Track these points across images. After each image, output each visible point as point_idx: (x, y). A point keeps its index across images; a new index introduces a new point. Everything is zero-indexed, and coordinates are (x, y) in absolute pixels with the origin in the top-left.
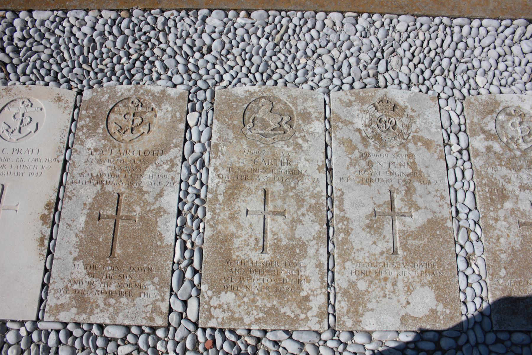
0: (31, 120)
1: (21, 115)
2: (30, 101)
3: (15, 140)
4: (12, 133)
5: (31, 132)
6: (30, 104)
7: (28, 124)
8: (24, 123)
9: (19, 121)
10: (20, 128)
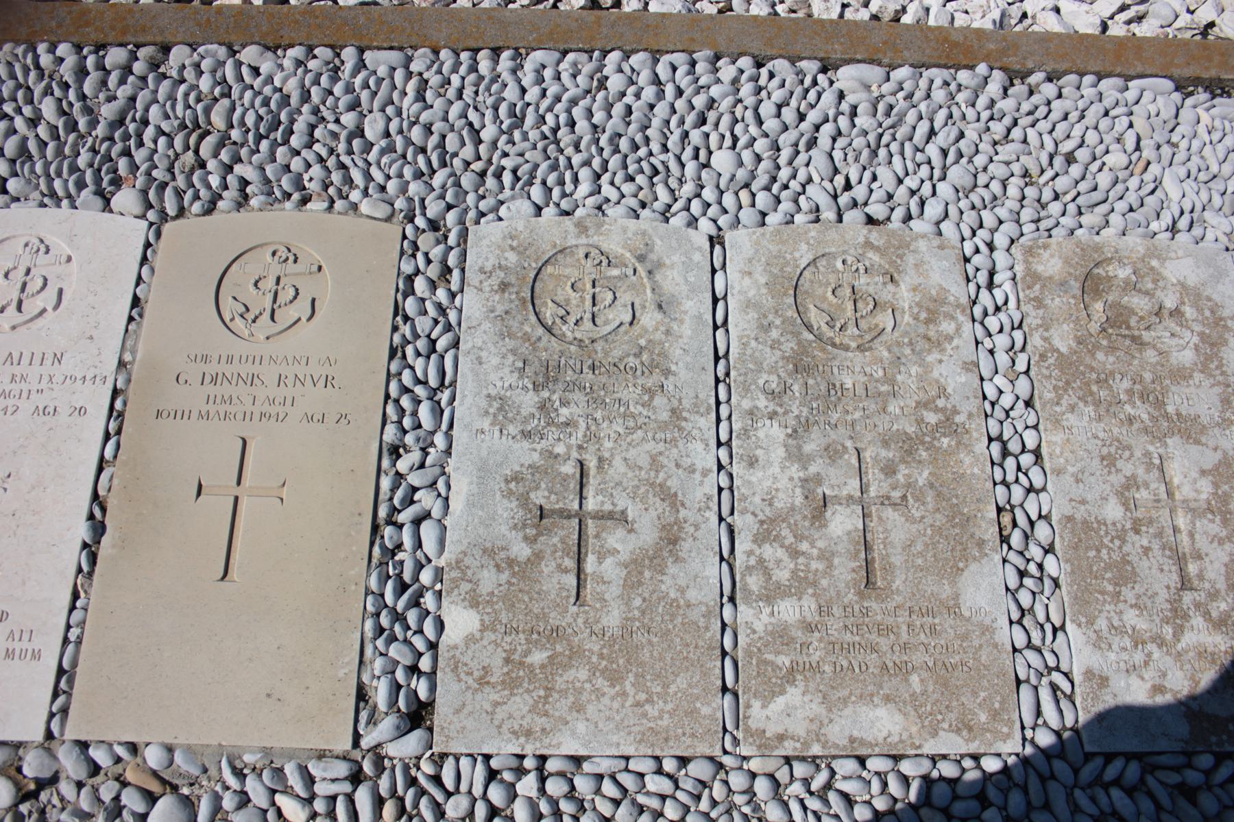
0: (297, 293)
2: (289, 250)
3: (262, 337)
4: (254, 321)
5: (299, 319)
6: (292, 258)
7: (291, 302)
8: (281, 300)
9: (270, 297)
10: (273, 311)
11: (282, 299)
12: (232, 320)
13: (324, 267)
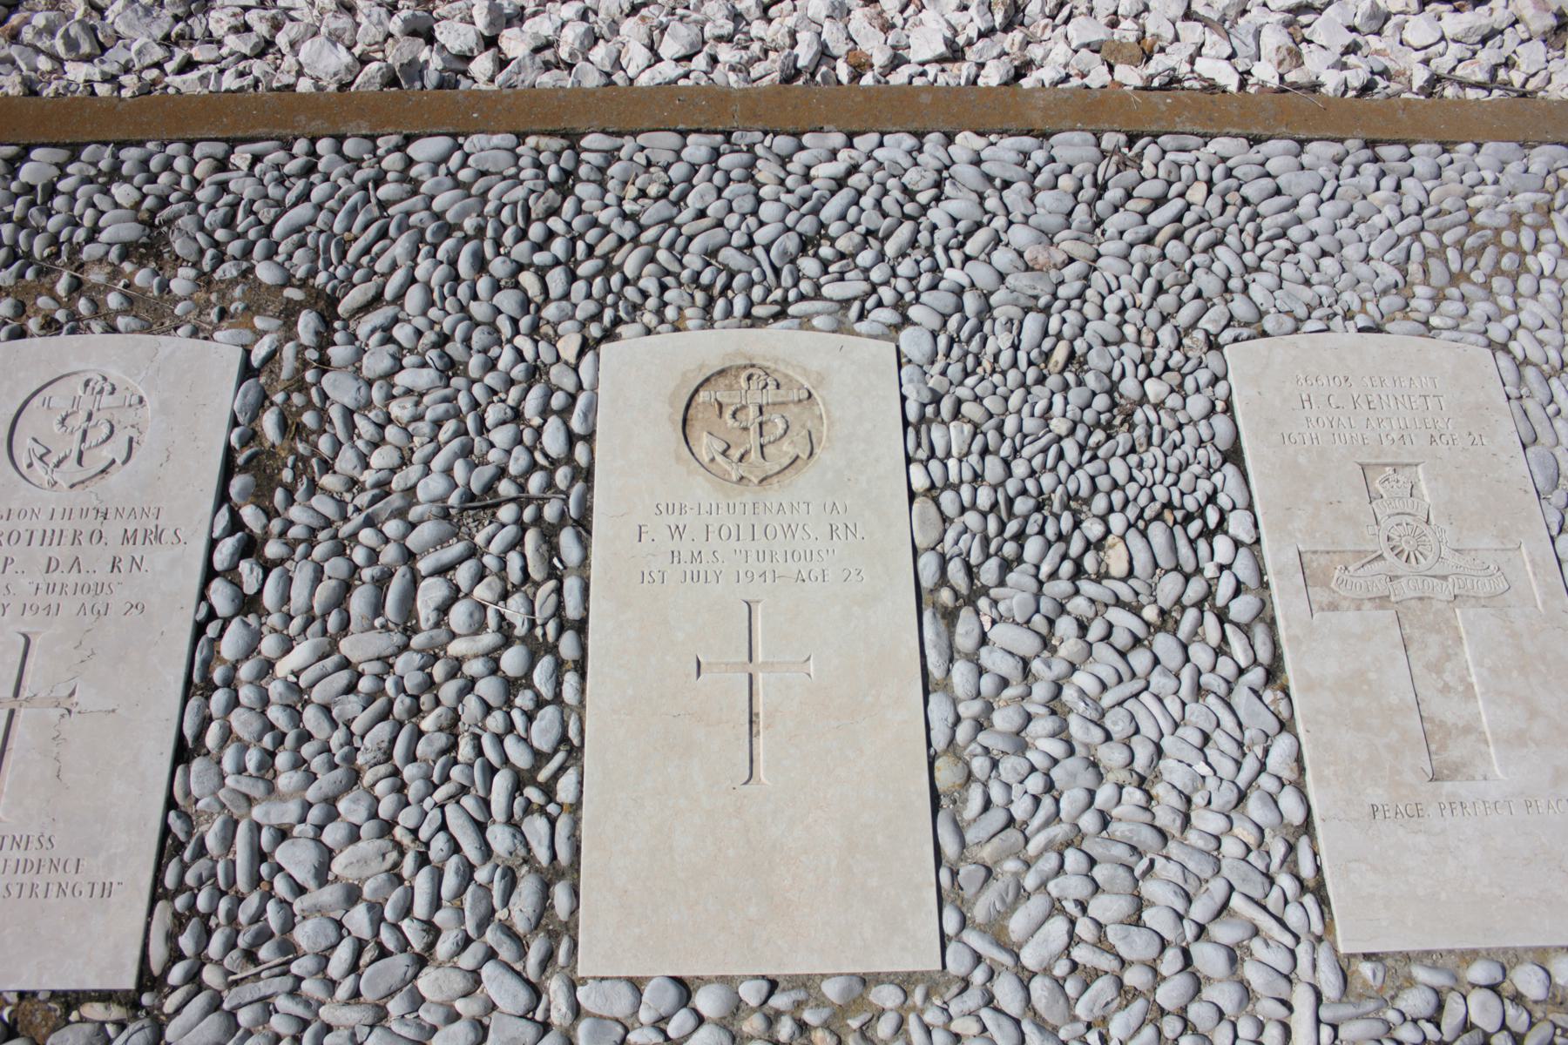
0: (112, 432)
1: (83, 415)
2: (105, 379)
3: (65, 486)
4: (57, 465)
5: (113, 462)
7: (104, 441)
9: (78, 435)
11: (93, 438)
12: (30, 465)
13: (146, 398)
